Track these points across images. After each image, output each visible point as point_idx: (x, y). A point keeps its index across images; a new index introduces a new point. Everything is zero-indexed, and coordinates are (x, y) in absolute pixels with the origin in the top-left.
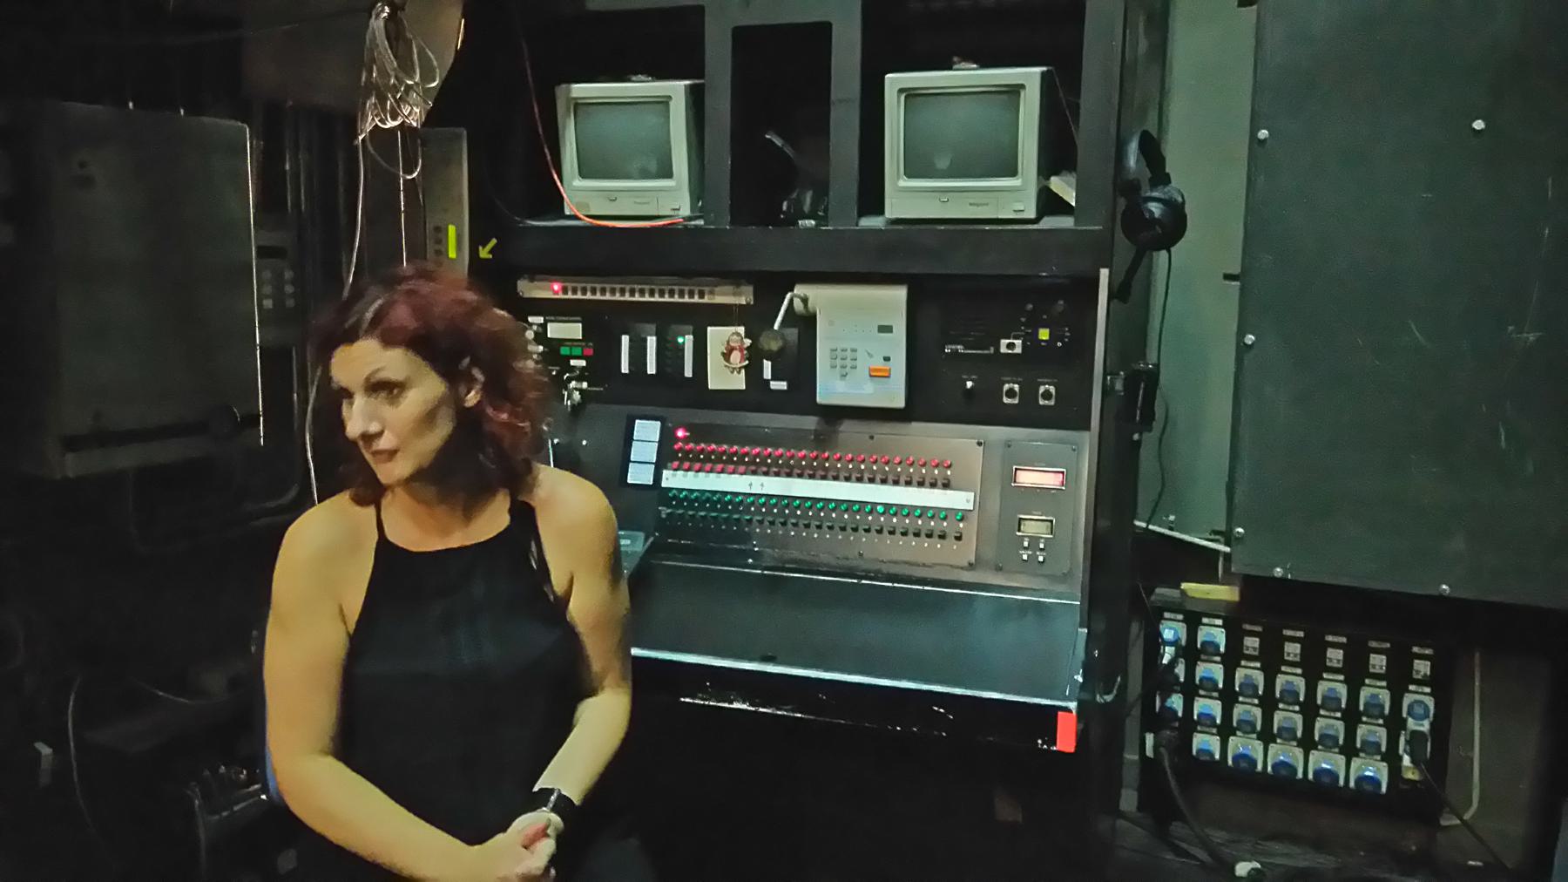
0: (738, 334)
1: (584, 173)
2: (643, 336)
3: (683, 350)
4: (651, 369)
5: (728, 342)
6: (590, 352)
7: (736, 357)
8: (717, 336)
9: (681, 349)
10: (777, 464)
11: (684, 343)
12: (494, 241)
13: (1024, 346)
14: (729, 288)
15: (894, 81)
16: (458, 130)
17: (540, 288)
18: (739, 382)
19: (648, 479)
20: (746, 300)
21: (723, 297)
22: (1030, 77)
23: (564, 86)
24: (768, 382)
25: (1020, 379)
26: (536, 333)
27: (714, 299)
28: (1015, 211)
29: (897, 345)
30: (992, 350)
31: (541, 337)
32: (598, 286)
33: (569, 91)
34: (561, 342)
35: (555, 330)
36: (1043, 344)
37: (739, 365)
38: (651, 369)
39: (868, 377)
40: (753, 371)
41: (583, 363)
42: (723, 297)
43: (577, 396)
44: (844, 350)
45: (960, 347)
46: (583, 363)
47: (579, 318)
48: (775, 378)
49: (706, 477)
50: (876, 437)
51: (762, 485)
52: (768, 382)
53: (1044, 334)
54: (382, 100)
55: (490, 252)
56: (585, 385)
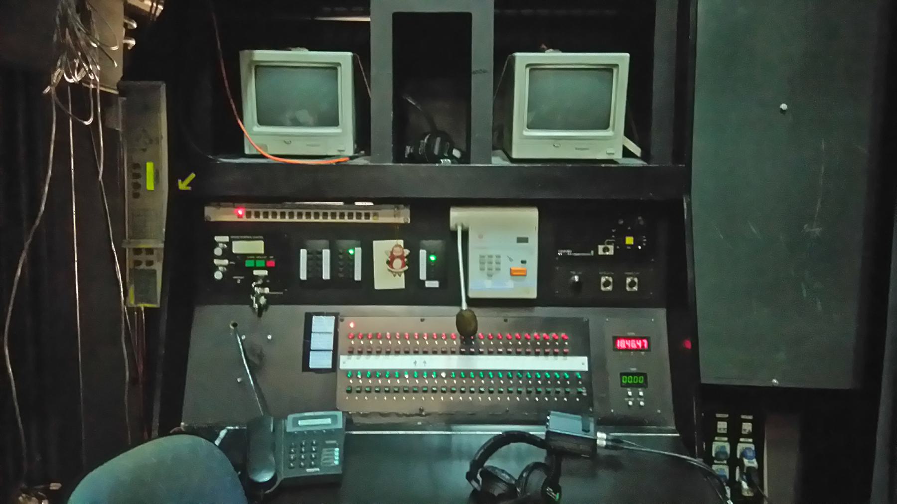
0: (400, 246)
1: (261, 122)
2: (320, 250)
3: (353, 260)
4: (326, 275)
5: (392, 253)
6: (272, 263)
7: (398, 263)
8: (382, 248)
9: (352, 259)
10: (526, 346)
11: (353, 255)
12: (193, 176)
13: (615, 250)
14: (391, 211)
15: (522, 59)
16: (160, 83)
17: (228, 214)
18: (399, 283)
19: (327, 363)
20: (404, 220)
21: (387, 216)
22: (622, 59)
23: (247, 51)
24: (423, 282)
25: (638, 273)
26: (224, 250)
27: (378, 219)
28: (607, 153)
29: (531, 253)
30: (592, 252)
31: (228, 253)
32: (270, 211)
33: (252, 55)
34: (245, 256)
35: (240, 247)
36: (629, 248)
37: (401, 270)
38: (326, 275)
39: (510, 276)
40: (412, 274)
41: (265, 273)
42: (387, 216)
43: (263, 300)
44: (491, 257)
45: (569, 252)
46: (265, 273)
47: (261, 237)
48: (429, 278)
49: (348, 359)
50: (508, 319)
51: (425, 362)
52: (423, 282)
53: (629, 240)
54: (72, 57)
55: (188, 185)
56: (267, 290)
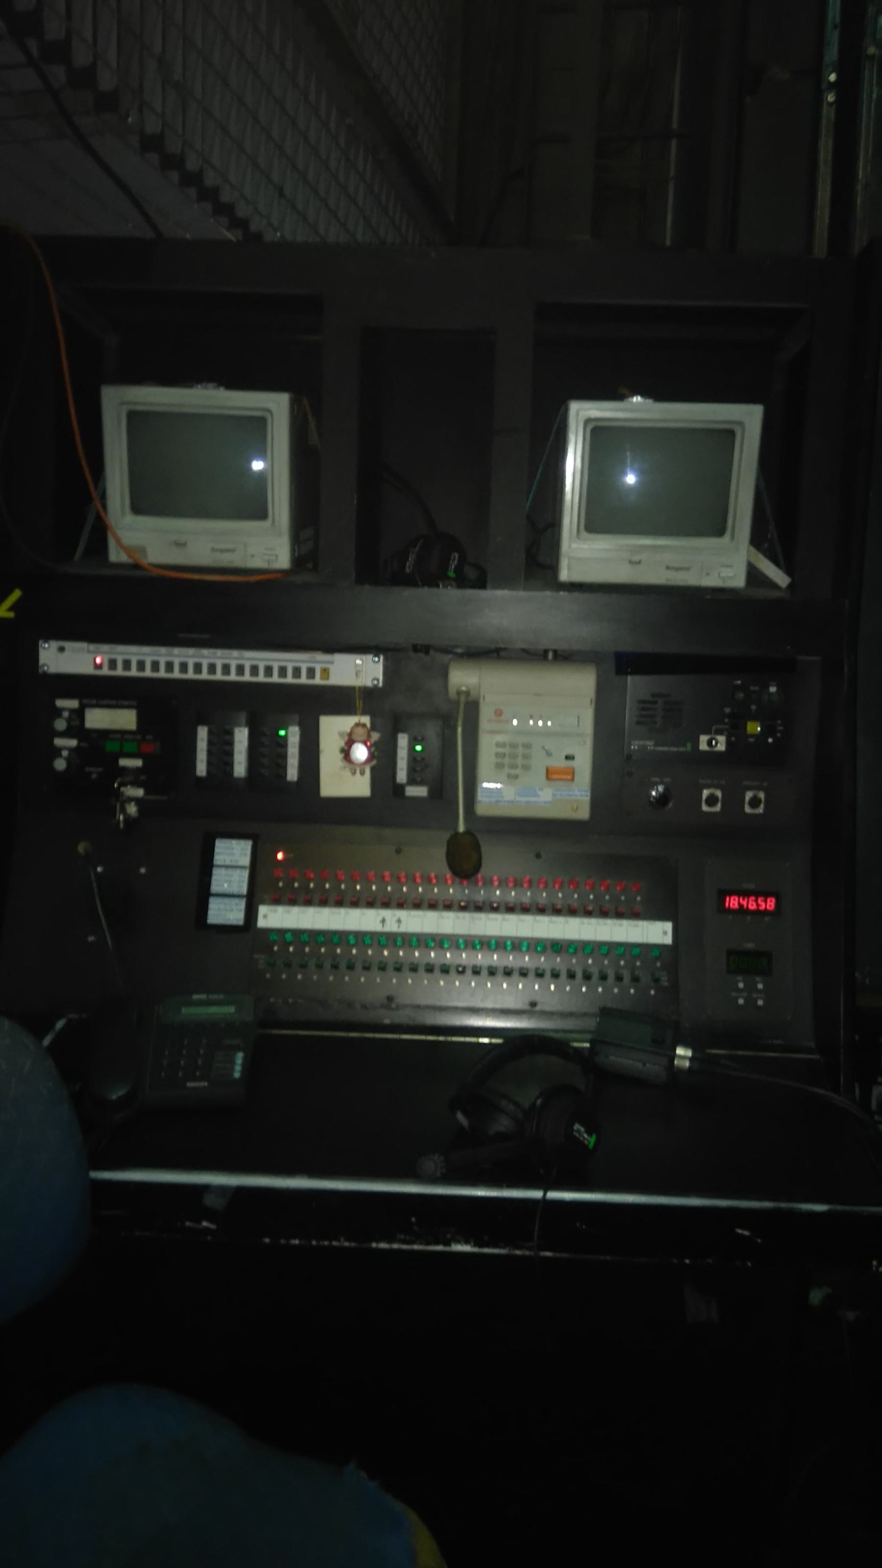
0: (364, 725)
1: (137, 509)
4: (240, 768)
9: (283, 743)
12: (17, 594)
26: (69, 720)
30: (689, 746)
31: (77, 728)
34: (105, 734)
36: (751, 740)
38: (240, 768)
41: (138, 763)
43: (132, 809)
46: (138, 763)
47: (134, 703)
55: (10, 609)
